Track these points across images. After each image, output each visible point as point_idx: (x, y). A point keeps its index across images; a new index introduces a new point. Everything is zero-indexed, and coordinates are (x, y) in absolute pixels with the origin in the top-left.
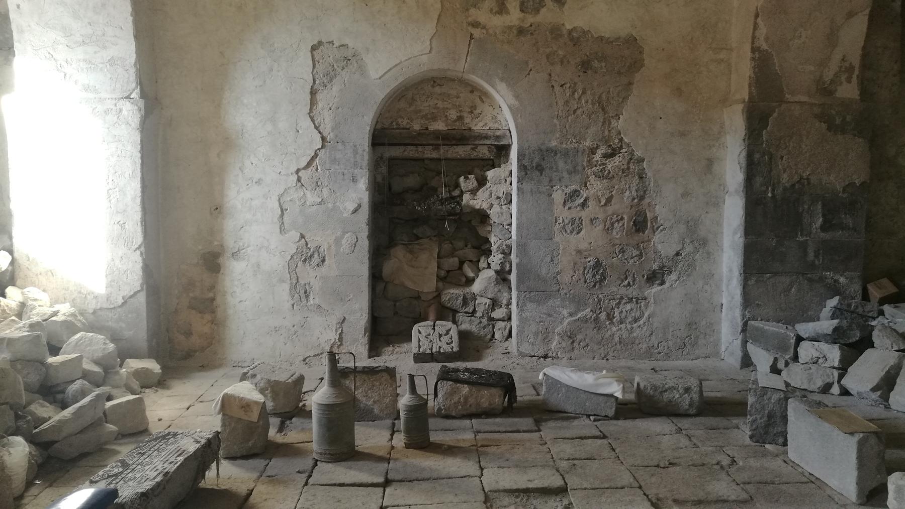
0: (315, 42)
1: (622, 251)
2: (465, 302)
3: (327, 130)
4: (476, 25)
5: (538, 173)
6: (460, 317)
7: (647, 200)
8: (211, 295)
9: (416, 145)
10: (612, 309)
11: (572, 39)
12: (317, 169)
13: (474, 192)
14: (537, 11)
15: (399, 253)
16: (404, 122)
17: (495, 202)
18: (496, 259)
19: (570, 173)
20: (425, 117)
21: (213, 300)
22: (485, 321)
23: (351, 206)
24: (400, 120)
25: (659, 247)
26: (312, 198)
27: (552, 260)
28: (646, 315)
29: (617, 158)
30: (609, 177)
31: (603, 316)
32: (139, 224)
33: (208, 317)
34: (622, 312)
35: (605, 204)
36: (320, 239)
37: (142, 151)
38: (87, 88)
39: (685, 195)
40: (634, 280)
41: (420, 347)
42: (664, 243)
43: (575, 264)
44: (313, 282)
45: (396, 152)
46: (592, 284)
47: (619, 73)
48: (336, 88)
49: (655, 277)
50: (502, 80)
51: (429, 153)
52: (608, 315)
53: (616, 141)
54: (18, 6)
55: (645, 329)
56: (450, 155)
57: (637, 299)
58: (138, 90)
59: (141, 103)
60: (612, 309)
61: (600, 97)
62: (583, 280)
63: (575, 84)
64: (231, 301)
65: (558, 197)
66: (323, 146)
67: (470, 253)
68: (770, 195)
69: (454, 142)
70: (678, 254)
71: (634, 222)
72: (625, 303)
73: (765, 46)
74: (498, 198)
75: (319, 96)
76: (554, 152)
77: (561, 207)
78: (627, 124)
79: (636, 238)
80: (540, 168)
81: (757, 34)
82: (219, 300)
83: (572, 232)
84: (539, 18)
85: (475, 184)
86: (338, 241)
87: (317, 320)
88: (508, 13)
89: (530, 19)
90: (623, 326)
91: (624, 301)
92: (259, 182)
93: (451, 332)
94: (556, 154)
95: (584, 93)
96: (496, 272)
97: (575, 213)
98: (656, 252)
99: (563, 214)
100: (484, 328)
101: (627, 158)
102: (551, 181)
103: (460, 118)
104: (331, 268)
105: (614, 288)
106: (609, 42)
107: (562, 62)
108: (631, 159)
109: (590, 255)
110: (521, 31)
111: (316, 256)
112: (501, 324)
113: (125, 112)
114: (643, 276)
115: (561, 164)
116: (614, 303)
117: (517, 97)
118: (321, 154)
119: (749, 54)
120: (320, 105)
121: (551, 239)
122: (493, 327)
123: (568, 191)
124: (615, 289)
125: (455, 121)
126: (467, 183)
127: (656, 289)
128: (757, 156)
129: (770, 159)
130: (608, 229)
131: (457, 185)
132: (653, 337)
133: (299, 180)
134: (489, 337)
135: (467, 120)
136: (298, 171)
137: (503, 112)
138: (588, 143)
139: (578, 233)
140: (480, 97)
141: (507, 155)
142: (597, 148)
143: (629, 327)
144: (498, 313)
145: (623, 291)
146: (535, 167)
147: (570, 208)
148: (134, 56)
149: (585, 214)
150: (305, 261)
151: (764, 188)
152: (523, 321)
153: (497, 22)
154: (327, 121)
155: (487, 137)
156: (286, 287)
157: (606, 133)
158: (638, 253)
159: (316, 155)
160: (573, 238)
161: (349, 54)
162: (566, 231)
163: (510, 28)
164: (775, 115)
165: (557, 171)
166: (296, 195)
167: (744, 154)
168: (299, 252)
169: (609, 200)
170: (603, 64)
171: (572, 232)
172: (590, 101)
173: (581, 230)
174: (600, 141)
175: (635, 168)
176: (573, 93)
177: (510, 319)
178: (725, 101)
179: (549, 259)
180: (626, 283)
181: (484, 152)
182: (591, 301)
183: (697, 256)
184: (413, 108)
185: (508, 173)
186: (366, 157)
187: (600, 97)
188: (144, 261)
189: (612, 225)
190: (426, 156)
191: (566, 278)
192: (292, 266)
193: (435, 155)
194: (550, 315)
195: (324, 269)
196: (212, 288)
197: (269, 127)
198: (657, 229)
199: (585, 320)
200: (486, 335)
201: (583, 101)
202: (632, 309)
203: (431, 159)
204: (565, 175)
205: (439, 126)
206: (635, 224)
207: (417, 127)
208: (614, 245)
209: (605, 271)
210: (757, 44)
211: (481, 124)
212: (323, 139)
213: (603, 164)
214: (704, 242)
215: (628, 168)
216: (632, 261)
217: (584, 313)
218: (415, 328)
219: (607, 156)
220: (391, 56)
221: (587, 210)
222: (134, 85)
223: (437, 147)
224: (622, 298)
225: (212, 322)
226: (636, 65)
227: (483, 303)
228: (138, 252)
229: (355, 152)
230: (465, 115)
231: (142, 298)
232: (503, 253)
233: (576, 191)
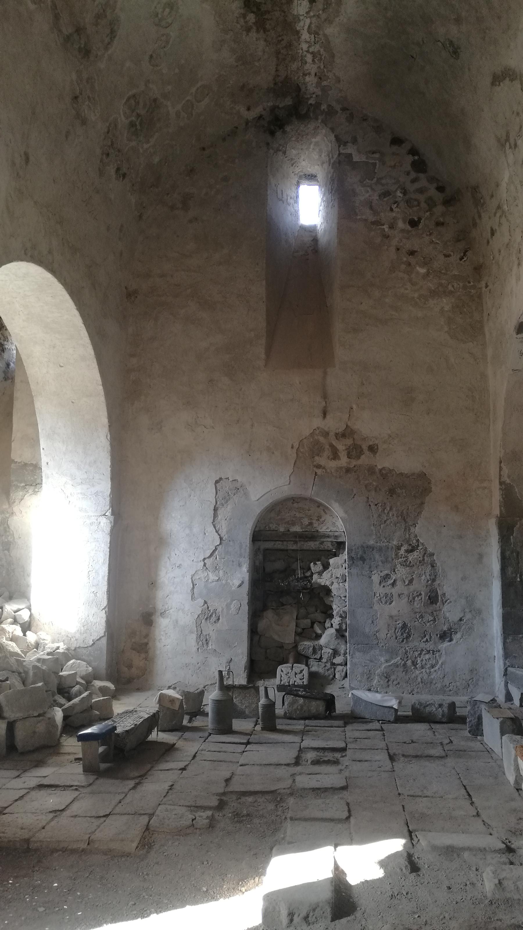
0: (218, 479)
1: (422, 617)
2: (314, 651)
3: (223, 532)
4: (319, 466)
5: (361, 562)
6: (311, 662)
7: (437, 582)
8: (146, 640)
9: (282, 541)
10: (416, 658)
11: (382, 475)
12: (216, 558)
13: (320, 573)
14: (358, 457)
15: (269, 614)
16: (273, 526)
17: (335, 581)
18: (336, 621)
19: (383, 562)
20: (288, 523)
21: (147, 644)
22: (328, 665)
23: (237, 583)
24: (271, 525)
25: (448, 615)
26: (212, 577)
27: (373, 622)
28: (440, 663)
29: (415, 553)
30: (410, 566)
31: (409, 663)
32: (106, 593)
33: (143, 655)
34: (422, 660)
35: (408, 584)
36: (217, 604)
37: (111, 548)
38: (81, 510)
39: (464, 578)
40: (431, 637)
41: (281, 680)
42: (451, 612)
43: (389, 625)
44: (211, 633)
45: (269, 545)
46: (401, 640)
47: (415, 496)
48: (229, 507)
49: (445, 636)
50: (336, 501)
51: (291, 546)
52: (413, 662)
53: (414, 541)
54: (47, 463)
55: (439, 673)
56: (305, 548)
57: (433, 651)
60: (416, 658)
61: (402, 512)
62: (394, 637)
63: (385, 504)
64: (159, 645)
65: (376, 578)
66: (220, 544)
67: (319, 616)
68: (518, 579)
69: (306, 540)
70: (461, 620)
71: (429, 597)
72: (425, 654)
73: (508, 481)
74: (337, 578)
75: (219, 512)
76: (373, 548)
77: (378, 585)
78: (422, 530)
79: (431, 608)
80: (363, 559)
81: (502, 473)
82: (150, 644)
83: (386, 603)
84: (359, 462)
85: (321, 568)
86: (228, 606)
88: (339, 459)
89: (354, 463)
90: (424, 670)
91: (424, 652)
92: (179, 566)
93: (304, 672)
94: (373, 550)
95: (391, 509)
96: (336, 630)
97: (388, 590)
98: (445, 618)
99: (380, 590)
100: (328, 670)
101: (422, 553)
102: (370, 568)
103: (311, 524)
104: (223, 624)
105: (416, 643)
106: (407, 476)
107: (376, 491)
108: (425, 554)
109: (399, 619)
110: (348, 470)
111: (214, 616)
112: (339, 668)
113: (102, 524)
114: (437, 635)
115: (377, 556)
116: (416, 654)
117: (346, 512)
118: (219, 548)
119: (498, 486)
120: (220, 517)
121: (372, 608)
122: (335, 669)
123: (382, 574)
124: (417, 644)
125: (308, 525)
126: (315, 567)
127: (446, 644)
128: (508, 553)
129: (518, 556)
130: (411, 601)
131: (309, 569)
132: (446, 679)
133: (205, 565)
134: (331, 676)
135: (315, 525)
136: (204, 559)
138: (395, 543)
139: (390, 604)
140: (324, 510)
141: (344, 549)
142: (402, 545)
143: (428, 671)
144: (338, 660)
145: (423, 645)
146: (360, 558)
147: (384, 586)
148: (110, 490)
149: (395, 591)
150: (206, 619)
151: (514, 575)
152: (354, 665)
153: (333, 464)
154: (223, 527)
155: (328, 537)
156: (194, 636)
157: (407, 536)
158: (432, 618)
159: (216, 549)
160: (387, 607)
161: (238, 485)
162: (382, 602)
163: (341, 468)
164: (518, 526)
165: (374, 560)
166: (202, 575)
167: (499, 551)
168: (203, 613)
169: (411, 581)
170: (404, 491)
171: (386, 603)
172: (395, 515)
173: (392, 601)
174: (403, 541)
175: (428, 560)
176: (384, 510)
177: (346, 664)
178: (488, 515)
179: (371, 622)
180: (425, 639)
181: (328, 545)
182: (400, 652)
183: (475, 622)
184: (279, 517)
185: (343, 561)
186: (248, 550)
187: (402, 512)
188: (107, 617)
189: (414, 598)
190: (289, 548)
191: (382, 635)
192: (198, 623)
193: (295, 547)
194: (371, 661)
195: (218, 625)
196: (147, 636)
197: (187, 531)
198: (446, 602)
199: (397, 666)
200: (329, 675)
201: (391, 515)
202: (430, 659)
203: (293, 550)
204: (380, 563)
205: (297, 529)
206: (430, 598)
207: (282, 529)
208: (416, 613)
209: (410, 631)
210: (502, 480)
211: (325, 528)
212: (221, 539)
213: (406, 557)
214: (479, 612)
215: (424, 560)
216: (429, 624)
217: (396, 660)
218: (279, 668)
220: (264, 486)
221: (396, 588)
222: (108, 507)
223: (296, 542)
224: (422, 650)
225: (146, 659)
226: (426, 491)
227: (327, 652)
228: (104, 611)
229: (241, 547)
230: (314, 521)
231: (104, 641)
232: (341, 616)
233: (387, 575)
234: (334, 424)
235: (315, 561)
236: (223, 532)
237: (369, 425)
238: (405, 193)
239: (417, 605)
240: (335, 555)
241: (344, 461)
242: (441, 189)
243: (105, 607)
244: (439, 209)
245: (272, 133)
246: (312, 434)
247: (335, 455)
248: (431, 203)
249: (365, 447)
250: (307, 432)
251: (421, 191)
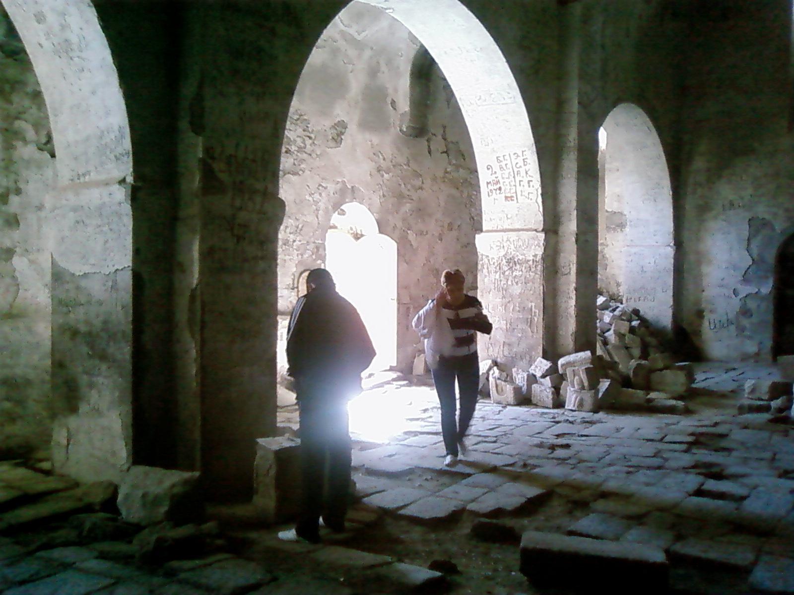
3: (755, 256)
36: (752, 305)
58: (673, 242)
59: (675, 247)
86: (759, 306)
87: (748, 342)
104: (755, 319)
212: (753, 260)
243: (671, 306)
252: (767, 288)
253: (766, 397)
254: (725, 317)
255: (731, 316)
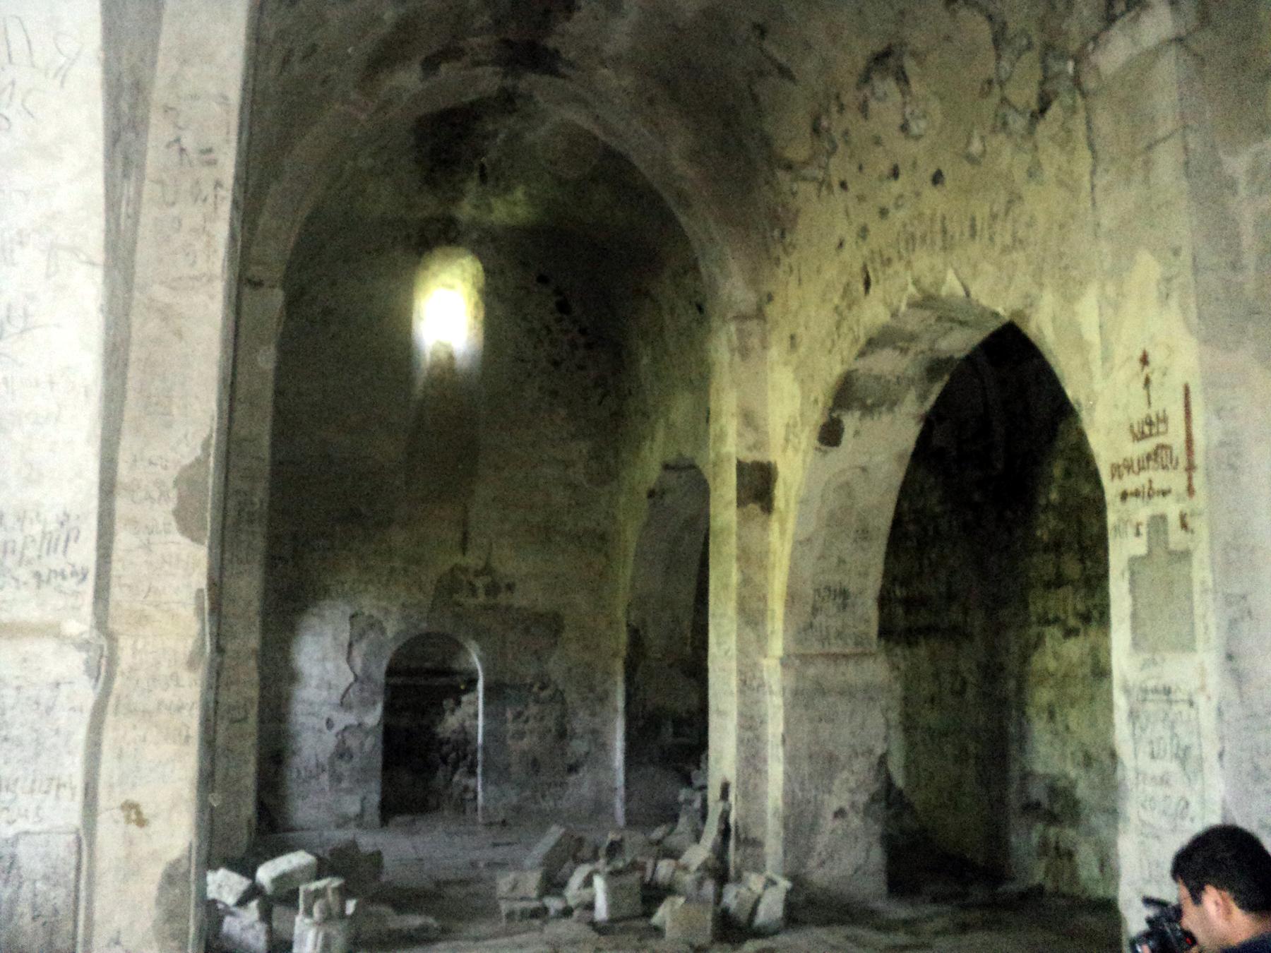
13: (453, 711)
31: (539, 795)
36: (353, 743)
42: (579, 747)
49: (573, 769)
86: (362, 744)
103: (444, 661)
117: (482, 650)
137: (474, 659)
144: (469, 796)
152: (486, 799)
153: (471, 602)
175: (558, 697)
178: (615, 655)
196: (276, 773)
199: (527, 799)
205: (428, 665)
207: (414, 665)
212: (356, 676)
219: (543, 688)
234: (472, 560)
235: (445, 697)
236: (358, 669)
237: (510, 564)
238: (549, 331)
239: (549, 738)
240: (466, 691)
241: (482, 598)
242: (583, 332)
244: (581, 353)
245: (420, 255)
246: (452, 570)
247: (473, 591)
248: (573, 345)
249: (502, 585)
250: (447, 568)
251: (566, 332)
252: (373, 717)
253: (534, 894)
254: (313, 762)
255: (323, 759)
